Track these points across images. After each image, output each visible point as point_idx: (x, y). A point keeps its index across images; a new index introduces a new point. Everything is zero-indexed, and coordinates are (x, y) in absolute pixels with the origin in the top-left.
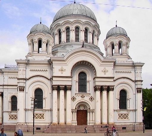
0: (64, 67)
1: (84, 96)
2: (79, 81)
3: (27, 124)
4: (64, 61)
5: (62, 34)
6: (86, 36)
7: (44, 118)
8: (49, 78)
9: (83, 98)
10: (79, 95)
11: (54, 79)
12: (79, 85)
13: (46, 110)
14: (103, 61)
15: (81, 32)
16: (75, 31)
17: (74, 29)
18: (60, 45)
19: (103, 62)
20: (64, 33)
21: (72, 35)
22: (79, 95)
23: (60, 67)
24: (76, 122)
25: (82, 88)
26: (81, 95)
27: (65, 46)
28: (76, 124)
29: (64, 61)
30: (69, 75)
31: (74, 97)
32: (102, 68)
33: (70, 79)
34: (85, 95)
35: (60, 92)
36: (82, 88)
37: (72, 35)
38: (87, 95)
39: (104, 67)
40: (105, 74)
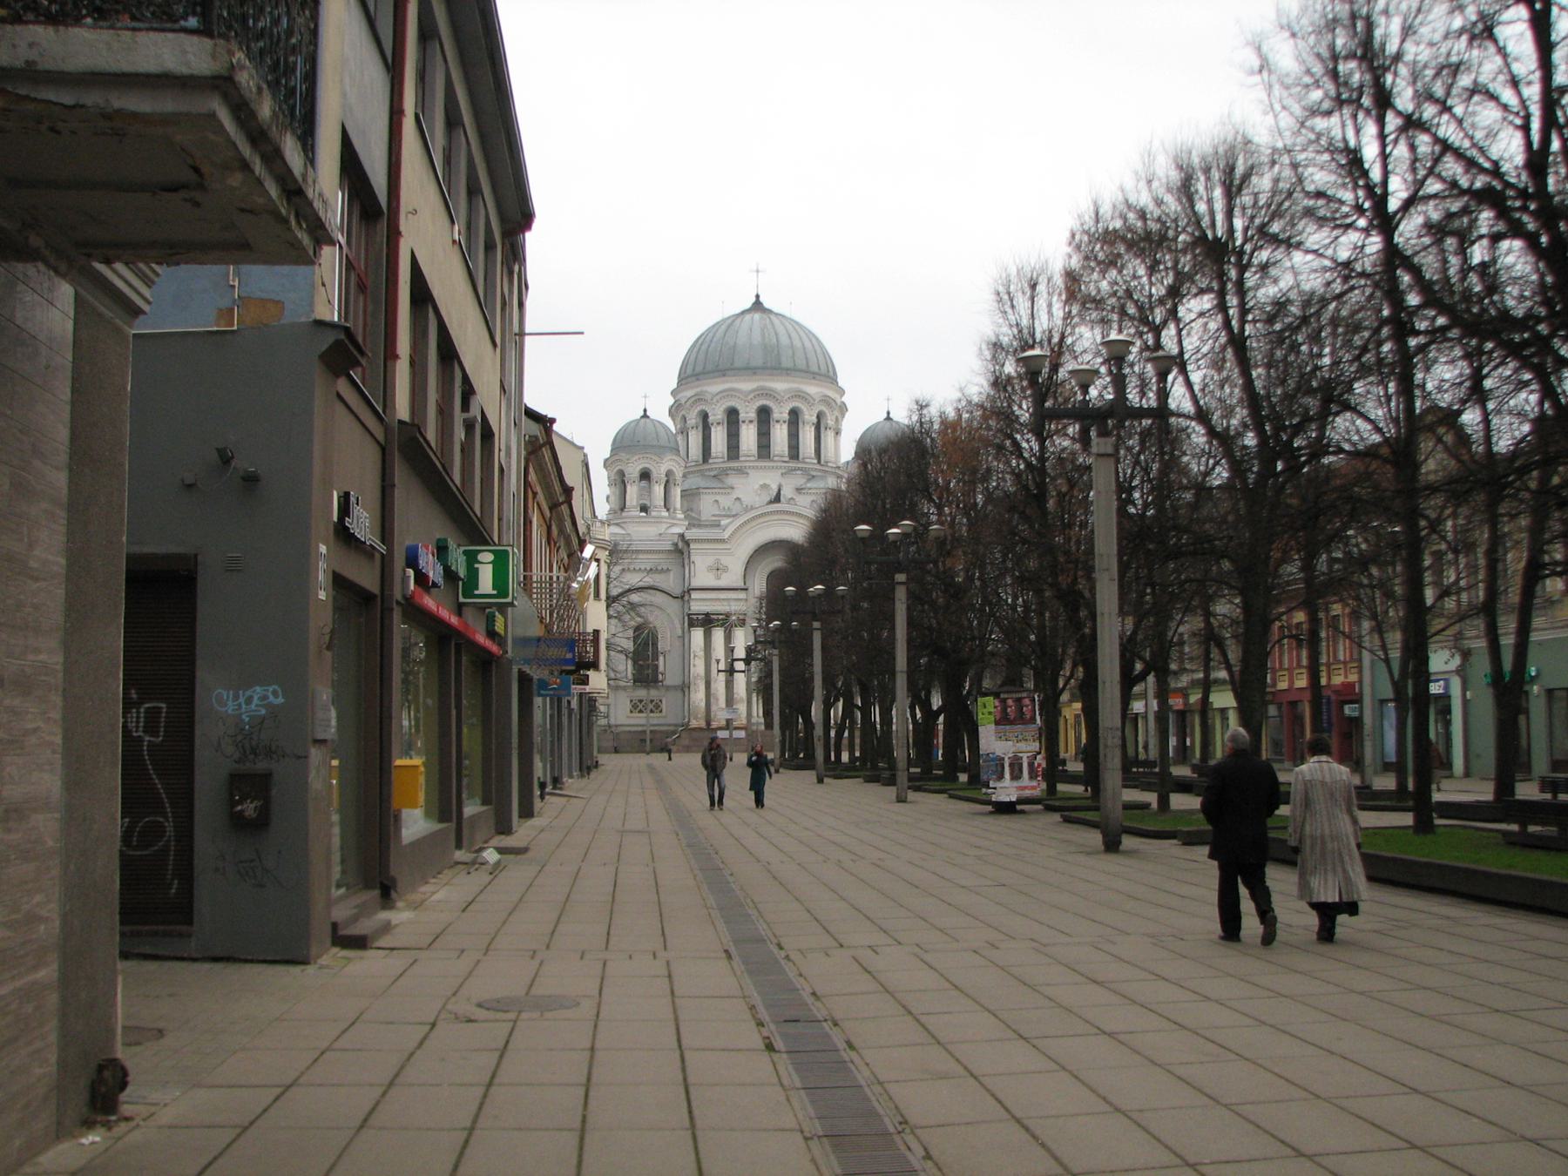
3: (613, 729)
5: (713, 429)
6: (794, 436)
7: (661, 711)
8: (677, 591)
13: (668, 688)
15: (778, 426)
16: (756, 423)
17: (753, 415)
18: (706, 467)
20: (720, 428)
21: (749, 436)
23: (710, 560)
24: (762, 720)
27: (725, 472)
28: (763, 727)
30: (740, 584)
33: (742, 595)
35: (713, 632)
37: (749, 436)
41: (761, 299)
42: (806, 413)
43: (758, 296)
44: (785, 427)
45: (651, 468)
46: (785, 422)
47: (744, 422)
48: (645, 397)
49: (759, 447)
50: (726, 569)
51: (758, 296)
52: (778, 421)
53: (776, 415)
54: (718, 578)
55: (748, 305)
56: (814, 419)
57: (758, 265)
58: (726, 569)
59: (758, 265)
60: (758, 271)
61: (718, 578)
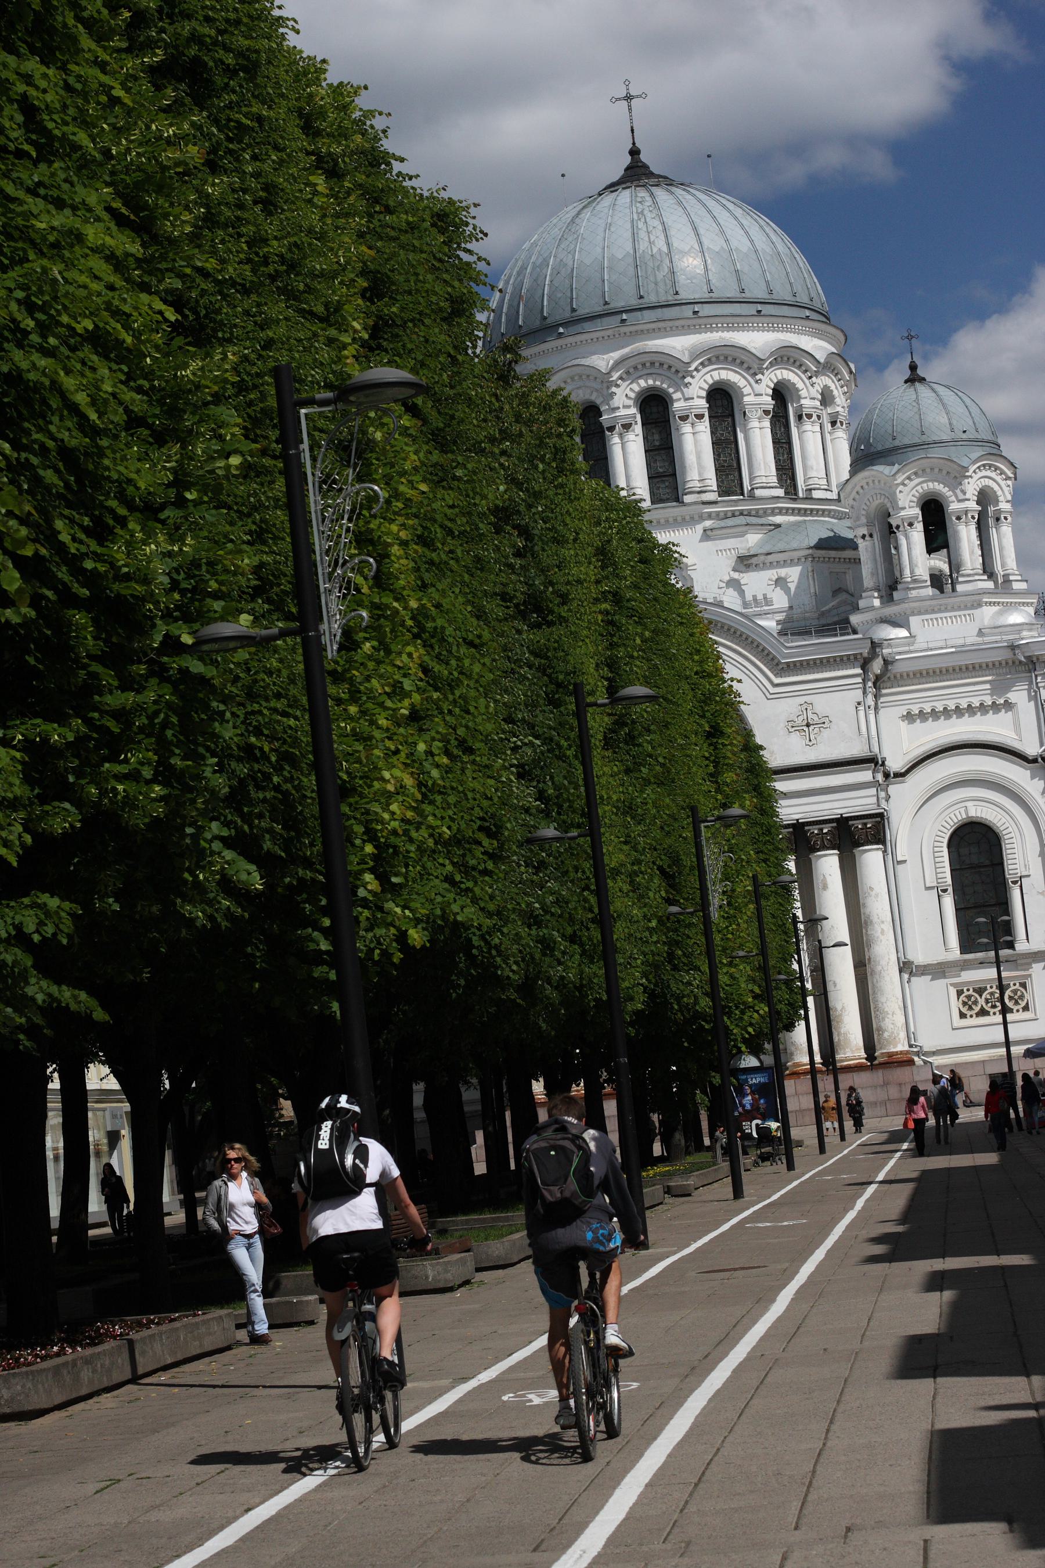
32: (789, 707)
40: (810, 743)
41: (643, 157)
42: (747, 390)
43: (634, 152)
44: (704, 428)
47: (611, 429)
49: (650, 478)
51: (634, 152)
52: (684, 418)
53: (678, 406)
55: (618, 173)
56: (768, 402)
57: (627, 83)
59: (627, 83)
60: (629, 98)
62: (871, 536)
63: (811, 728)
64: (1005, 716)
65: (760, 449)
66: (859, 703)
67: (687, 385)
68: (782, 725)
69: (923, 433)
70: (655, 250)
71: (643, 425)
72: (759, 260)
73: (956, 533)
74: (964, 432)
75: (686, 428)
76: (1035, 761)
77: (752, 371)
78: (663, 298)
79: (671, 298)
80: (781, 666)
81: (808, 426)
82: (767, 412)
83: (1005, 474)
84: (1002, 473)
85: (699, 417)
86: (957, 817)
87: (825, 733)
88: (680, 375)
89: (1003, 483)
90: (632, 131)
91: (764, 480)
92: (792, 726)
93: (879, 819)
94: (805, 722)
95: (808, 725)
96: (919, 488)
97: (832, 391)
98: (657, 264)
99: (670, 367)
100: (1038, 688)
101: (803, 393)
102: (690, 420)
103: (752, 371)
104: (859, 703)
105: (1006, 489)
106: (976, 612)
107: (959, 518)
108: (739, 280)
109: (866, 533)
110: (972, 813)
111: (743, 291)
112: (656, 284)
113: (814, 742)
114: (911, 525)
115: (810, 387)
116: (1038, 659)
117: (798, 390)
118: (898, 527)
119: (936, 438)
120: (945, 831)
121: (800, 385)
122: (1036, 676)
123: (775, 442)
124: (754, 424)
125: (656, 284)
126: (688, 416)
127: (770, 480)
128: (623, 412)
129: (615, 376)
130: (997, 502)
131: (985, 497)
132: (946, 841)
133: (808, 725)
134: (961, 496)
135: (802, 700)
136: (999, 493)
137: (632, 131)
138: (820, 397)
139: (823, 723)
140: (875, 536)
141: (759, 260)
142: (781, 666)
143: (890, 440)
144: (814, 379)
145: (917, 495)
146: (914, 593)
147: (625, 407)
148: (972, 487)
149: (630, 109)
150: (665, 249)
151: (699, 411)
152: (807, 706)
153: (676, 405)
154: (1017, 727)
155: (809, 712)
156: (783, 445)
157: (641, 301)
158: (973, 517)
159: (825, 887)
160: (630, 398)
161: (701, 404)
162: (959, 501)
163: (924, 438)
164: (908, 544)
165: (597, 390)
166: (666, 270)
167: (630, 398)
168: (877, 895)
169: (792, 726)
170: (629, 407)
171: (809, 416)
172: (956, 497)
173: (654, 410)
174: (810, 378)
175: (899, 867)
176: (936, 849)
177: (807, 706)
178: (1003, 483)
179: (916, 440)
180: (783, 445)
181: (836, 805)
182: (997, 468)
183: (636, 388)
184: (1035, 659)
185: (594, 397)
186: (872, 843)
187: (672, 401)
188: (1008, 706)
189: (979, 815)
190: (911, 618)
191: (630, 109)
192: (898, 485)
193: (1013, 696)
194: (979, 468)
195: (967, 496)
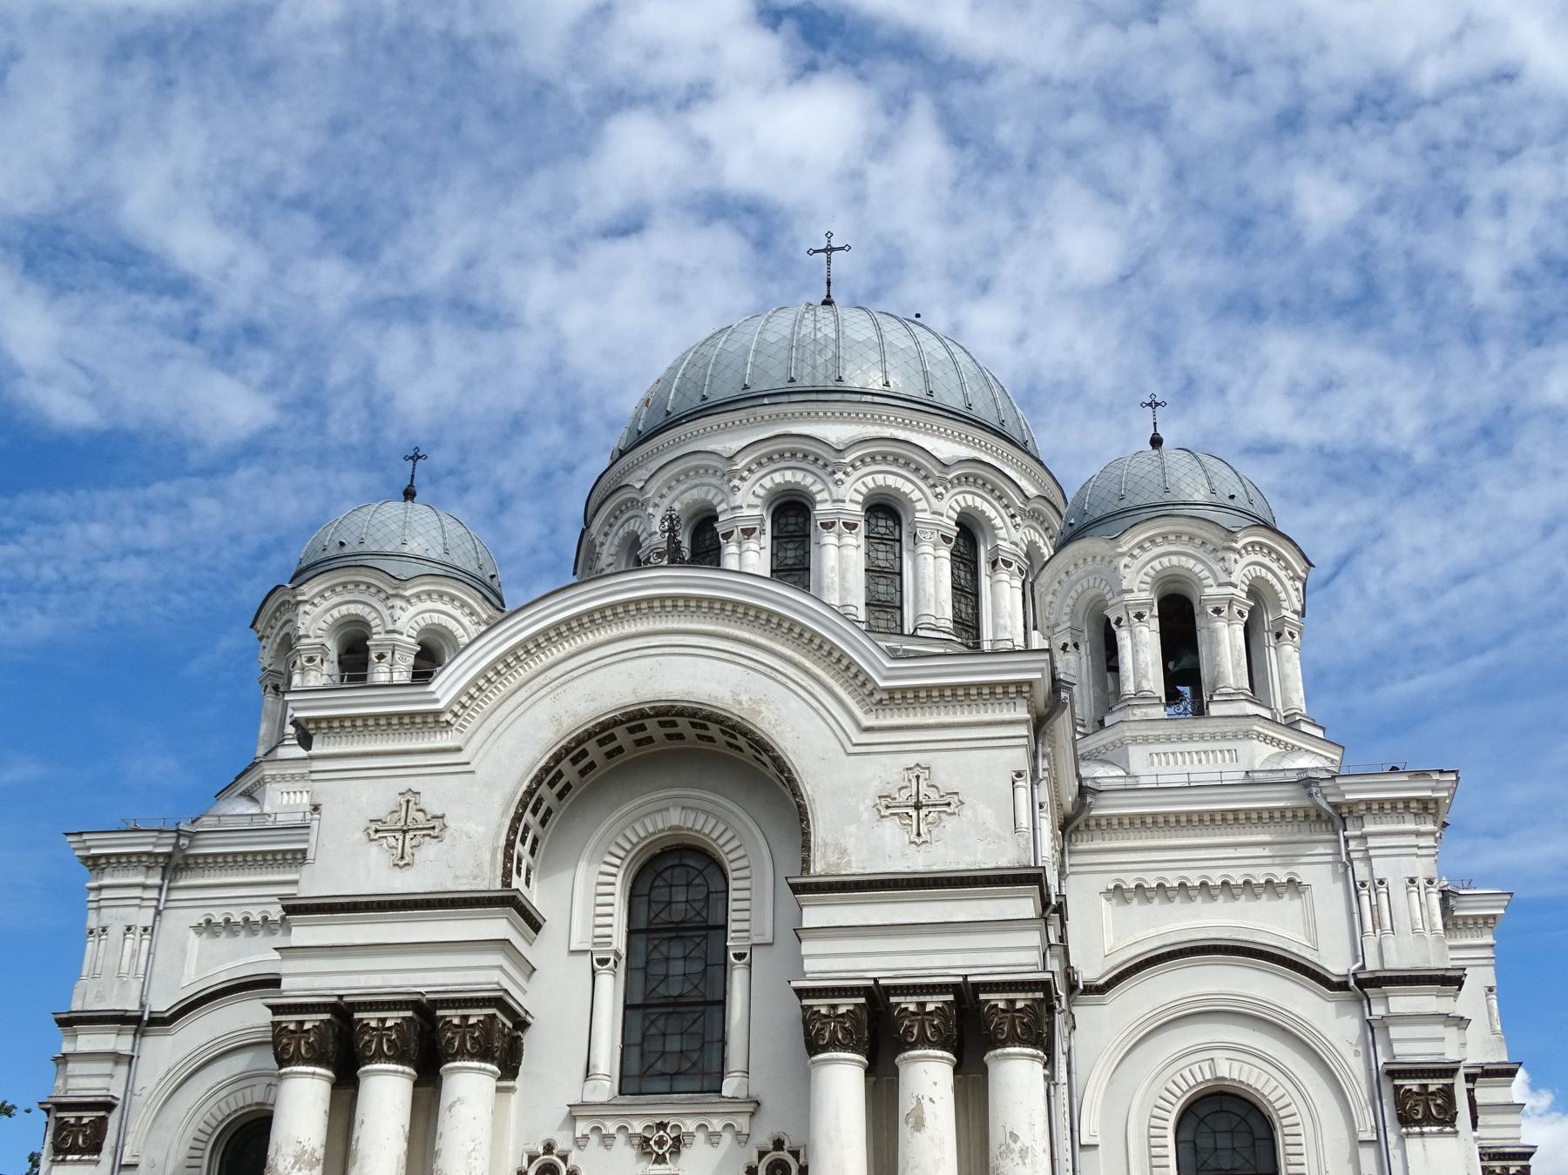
0: (435, 794)
1: (678, 1143)
2: (639, 961)
4: (432, 721)
9: (660, 1159)
10: (611, 1127)
11: (305, 933)
12: (627, 1007)
14: (890, 691)
15: (830, 539)
16: (766, 540)
19: (897, 698)
22: (611, 1127)
25: (674, 1044)
26: (637, 1127)
29: (432, 721)
30: (490, 882)
31: (549, 1148)
32: (885, 771)
34: (689, 1125)
36: (674, 1044)
38: (716, 1124)
39: (911, 760)
40: (918, 842)
45: (371, 617)
46: (851, 526)
47: (727, 536)
48: (415, 457)
50: (434, 828)
52: (828, 526)
53: (823, 509)
54: (402, 862)
57: (829, 235)
58: (434, 828)
59: (829, 235)
60: (829, 250)
61: (402, 862)
62: (1076, 646)
63: (923, 812)
64: (1289, 906)
65: (932, 583)
66: (1019, 775)
67: (838, 483)
68: (869, 803)
69: (1167, 490)
70: (819, 335)
71: (773, 538)
72: (959, 373)
73: (1213, 633)
74: (1232, 497)
75: (830, 539)
76: (1342, 986)
77: (931, 481)
78: (821, 383)
79: (831, 385)
80: (877, 696)
81: (1003, 575)
82: (946, 539)
83: (1294, 570)
84: (1288, 567)
85: (851, 526)
86: (1195, 1076)
87: (950, 823)
88: (829, 469)
89: (1288, 583)
90: (829, 283)
91: (933, 620)
92: (887, 805)
93: (1040, 995)
94: (912, 801)
95: (918, 807)
96: (1156, 564)
97: (1039, 548)
98: (819, 348)
99: (817, 460)
100: (1351, 862)
101: (1002, 533)
102: (836, 528)
103: (931, 481)
104: (1019, 775)
105: (1293, 594)
106: (1243, 747)
107: (1217, 611)
108: (927, 381)
109: (1068, 640)
110: (1224, 1070)
111: (930, 394)
112: (814, 367)
113: (924, 837)
114: (1139, 616)
115: (1013, 530)
116: (1350, 812)
117: (989, 519)
118: (1119, 621)
119: (1183, 498)
120: (1173, 1100)
121: (998, 522)
122: (1346, 841)
123: (957, 589)
124: (926, 548)
125: (814, 367)
126: (833, 524)
127: (941, 623)
128: (746, 512)
129: (741, 463)
130: (1278, 605)
131: (1258, 593)
132: (1171, 1125)
133: (918, 807)
134: (1223, 578)
135: (911, 760)
136: (1283, 596)
137: (829, 283)
138: (1025, 549)
139: (948, 803)
140: (1082, 647)
141: (959, 373)
142: (877, 696)
143: (1115, 501)
144: (1018, 519)
145: (1152, 573)
146: (1139, 713)
147: (749, 506)
148: (1242, 569)
149: (829, 262)
150: (833, 335)
151: (851, 519)
152: (918, 772)
153: (818, 507)
154: (1311, 925)
155: (923, 784)
156: (967, 592)
157: (790, 385)
158: (1240, 613)
159: (919, 1125)
160: (758, 496)
161: (856, 510)
162: (1220, 585)
163: (1168, 497)
164: (1134, 645)
165: (715, 487)
166: (830, 354)
167: (758, 496)
168: (1023, 1153)
169: (887, 805)
170: (755, 506)
171: (1008, 564)
172: (1216, 578)
173: (792, 520)
174: (1013, 516)
175: (1083, 1157)
176: (1154, 1132)
177: (918, 772)
178: (1288, 583)
179: (1155, 499)
180: (967, 592)
181: (957, 959)
182: (1280, 558)
183: (767, 482)
184: (1345, 810)
185: (712, 496)
186: (1023, 1043)
187: (814, 502)
188: (1294, 885)
189: (1235, 1076)
190: (1131, 749)
191: (829, 262)
192: (1122, 555)
193: (1304, 874)
194: (1253, 544)
195: (1233, 579)
